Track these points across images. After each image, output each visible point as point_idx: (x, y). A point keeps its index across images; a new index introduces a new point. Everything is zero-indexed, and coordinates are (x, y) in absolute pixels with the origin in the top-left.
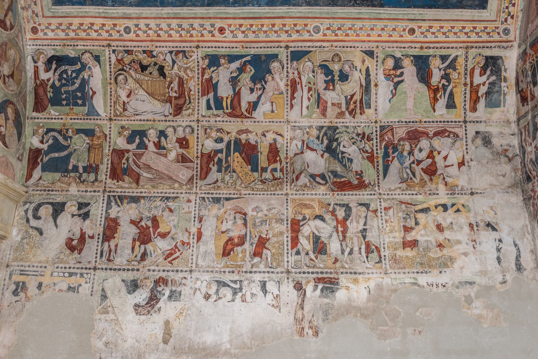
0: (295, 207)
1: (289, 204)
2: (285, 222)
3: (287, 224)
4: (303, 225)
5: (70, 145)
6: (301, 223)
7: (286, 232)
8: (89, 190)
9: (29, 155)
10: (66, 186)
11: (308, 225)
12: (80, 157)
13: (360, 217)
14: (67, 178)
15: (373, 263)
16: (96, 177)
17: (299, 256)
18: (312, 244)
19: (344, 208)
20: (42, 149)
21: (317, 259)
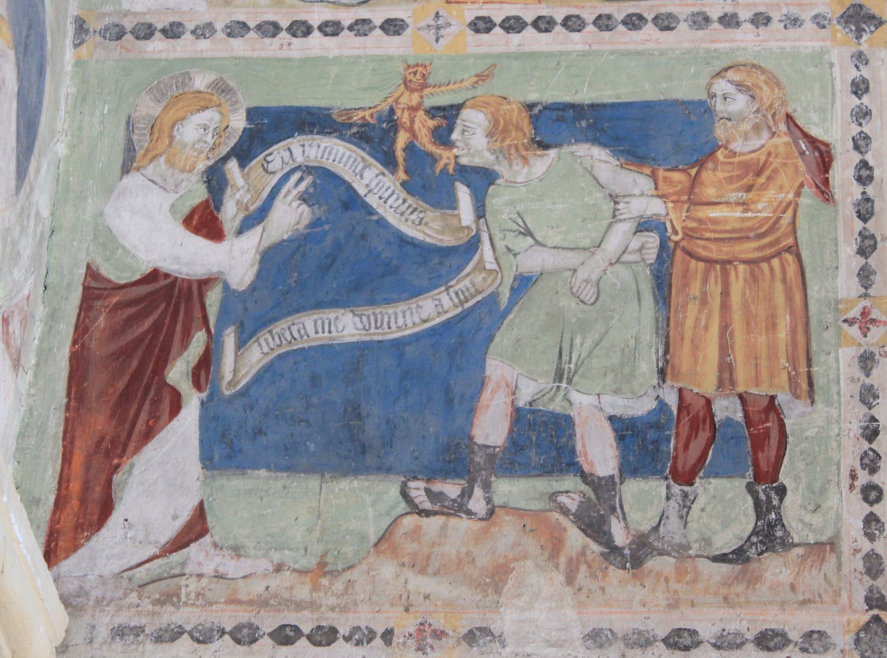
5: (473, 245)
8: (707, 631)
9: (81, 330)
10: (466, 594)
12: (582, 345)
14: (462, 524)
16: (761, 509)
20: (205, 284)
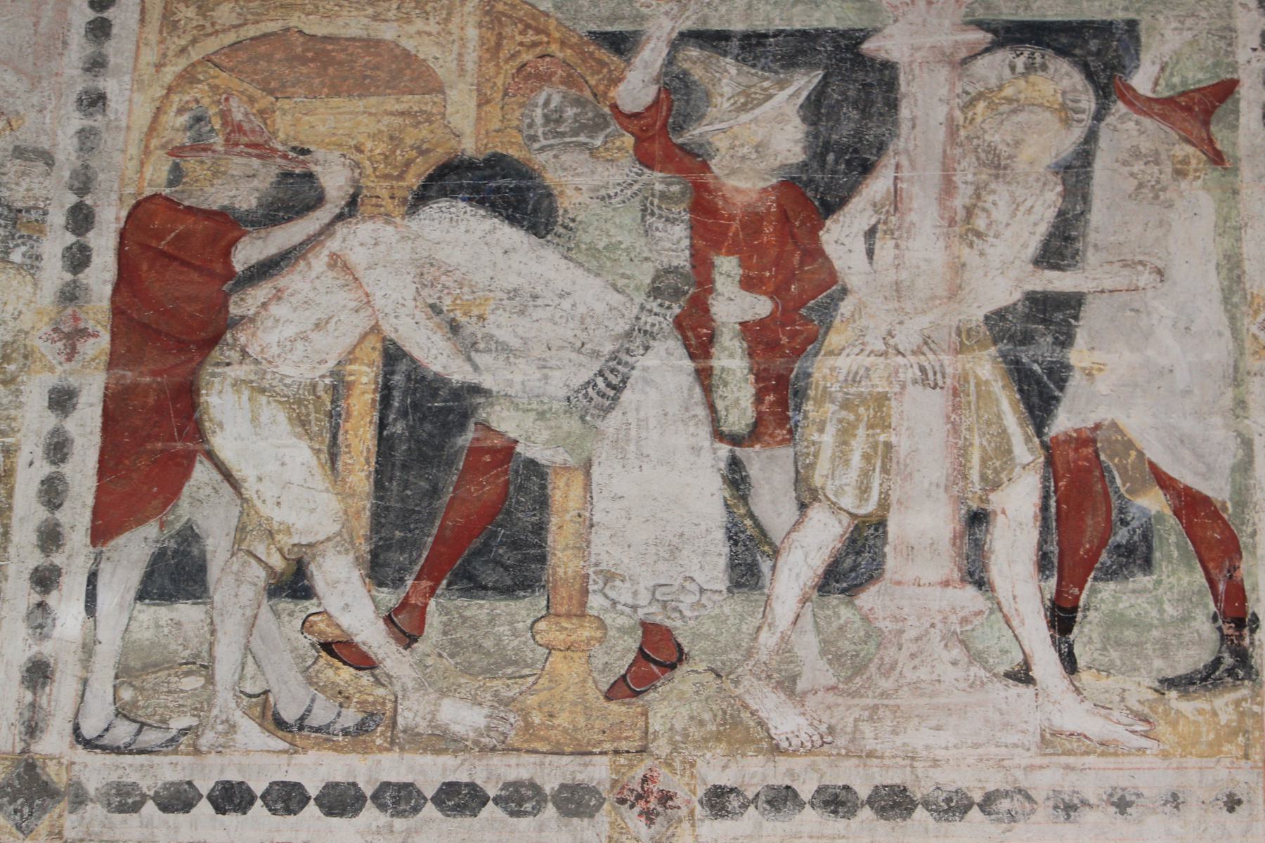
0: (188, 78)
1: (118, 49)
2: (55, 243)
3: (78, 259)
4: (266, 270)
6: (246, 254)
7: (50, 350)
11: (336, 262)
13: (997, 165)
15: (1139, 690)
17: (188, 613)
18: (360, 475)
19: (804, 82)
21: (408, 638)
